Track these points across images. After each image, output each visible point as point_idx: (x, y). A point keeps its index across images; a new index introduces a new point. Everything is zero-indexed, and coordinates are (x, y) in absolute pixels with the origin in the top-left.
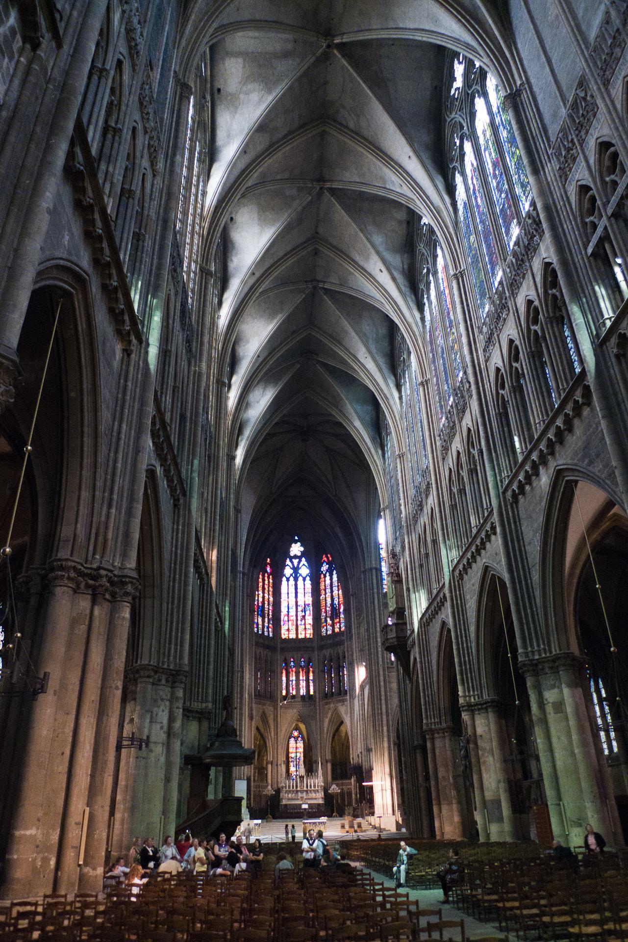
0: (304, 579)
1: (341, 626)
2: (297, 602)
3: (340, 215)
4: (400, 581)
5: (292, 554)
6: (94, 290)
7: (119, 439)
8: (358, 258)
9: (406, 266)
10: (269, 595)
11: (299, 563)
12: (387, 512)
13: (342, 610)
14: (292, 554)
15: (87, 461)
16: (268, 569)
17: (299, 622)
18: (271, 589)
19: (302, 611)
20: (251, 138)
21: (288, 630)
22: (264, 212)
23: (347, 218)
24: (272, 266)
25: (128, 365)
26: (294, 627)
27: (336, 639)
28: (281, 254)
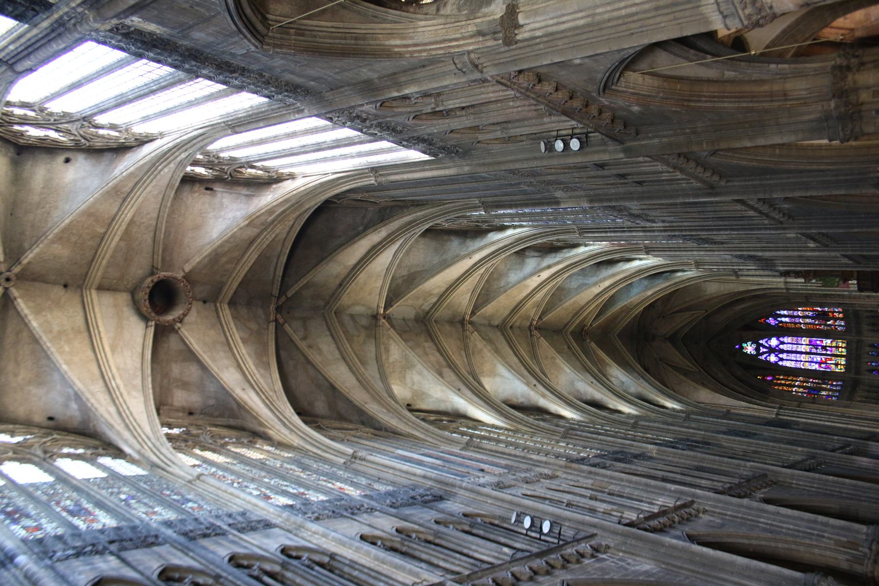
0: (783, 343)
1: (838, 312)
2: (806, 353)
3: (489, 309)
4: (815, 271)
5: (754, 352)
6: (687, 529)
7: (771, 525)
8: (525, 294)
9: (536, 254)
10: (797, 381)
11: (764, 347)
12: (740, 273)
13: (819, 309)
14: (754, 352)
15: (793, 547)
16: (769, 378)
17: (828, 352)
18: (790, 378)
19: (817, 349)
20: (448, 383)
21: (837, 365)
22: (483, 372)
23: (493, 303)
24: (526, 368)
25: (714, 512)
26: (833, 358)
27: (852, 316)
28: (515, 359)
